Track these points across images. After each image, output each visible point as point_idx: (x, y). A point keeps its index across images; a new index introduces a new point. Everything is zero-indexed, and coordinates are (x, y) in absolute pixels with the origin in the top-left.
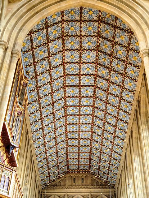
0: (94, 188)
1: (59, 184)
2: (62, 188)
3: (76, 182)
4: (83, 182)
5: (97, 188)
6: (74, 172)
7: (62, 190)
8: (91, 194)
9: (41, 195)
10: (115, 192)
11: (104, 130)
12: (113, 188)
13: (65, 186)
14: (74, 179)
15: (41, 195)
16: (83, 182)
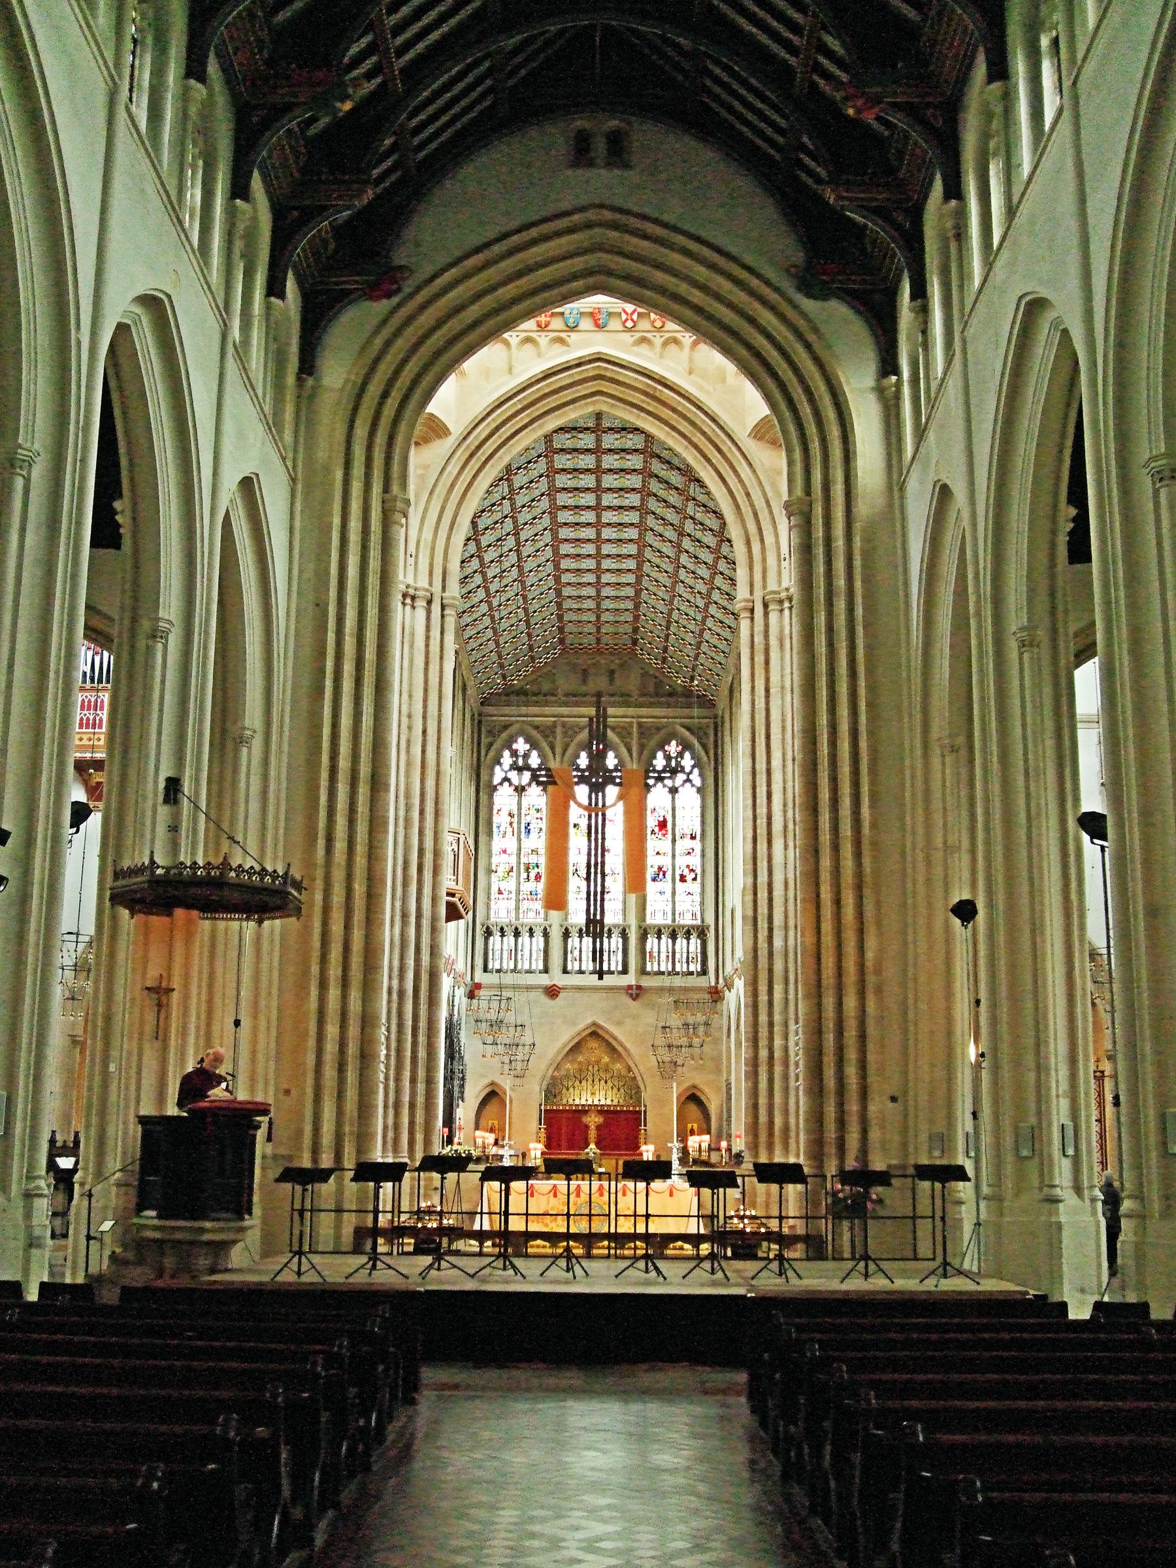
0: (651, 705)
1: (535, 688)
2: (547, 704)
3: (591, 679)
4: (612, 680)
5: (660, 705)
6: (579, 650)
7: (547, 710)
8: (640, 725)
9: (480, 722)
10: (716, 717)
11: (681, 534)
12: (712, 704)
13: (553, 695)
14: (585, 673)
15: (480, 722)
16: (612, 680)
